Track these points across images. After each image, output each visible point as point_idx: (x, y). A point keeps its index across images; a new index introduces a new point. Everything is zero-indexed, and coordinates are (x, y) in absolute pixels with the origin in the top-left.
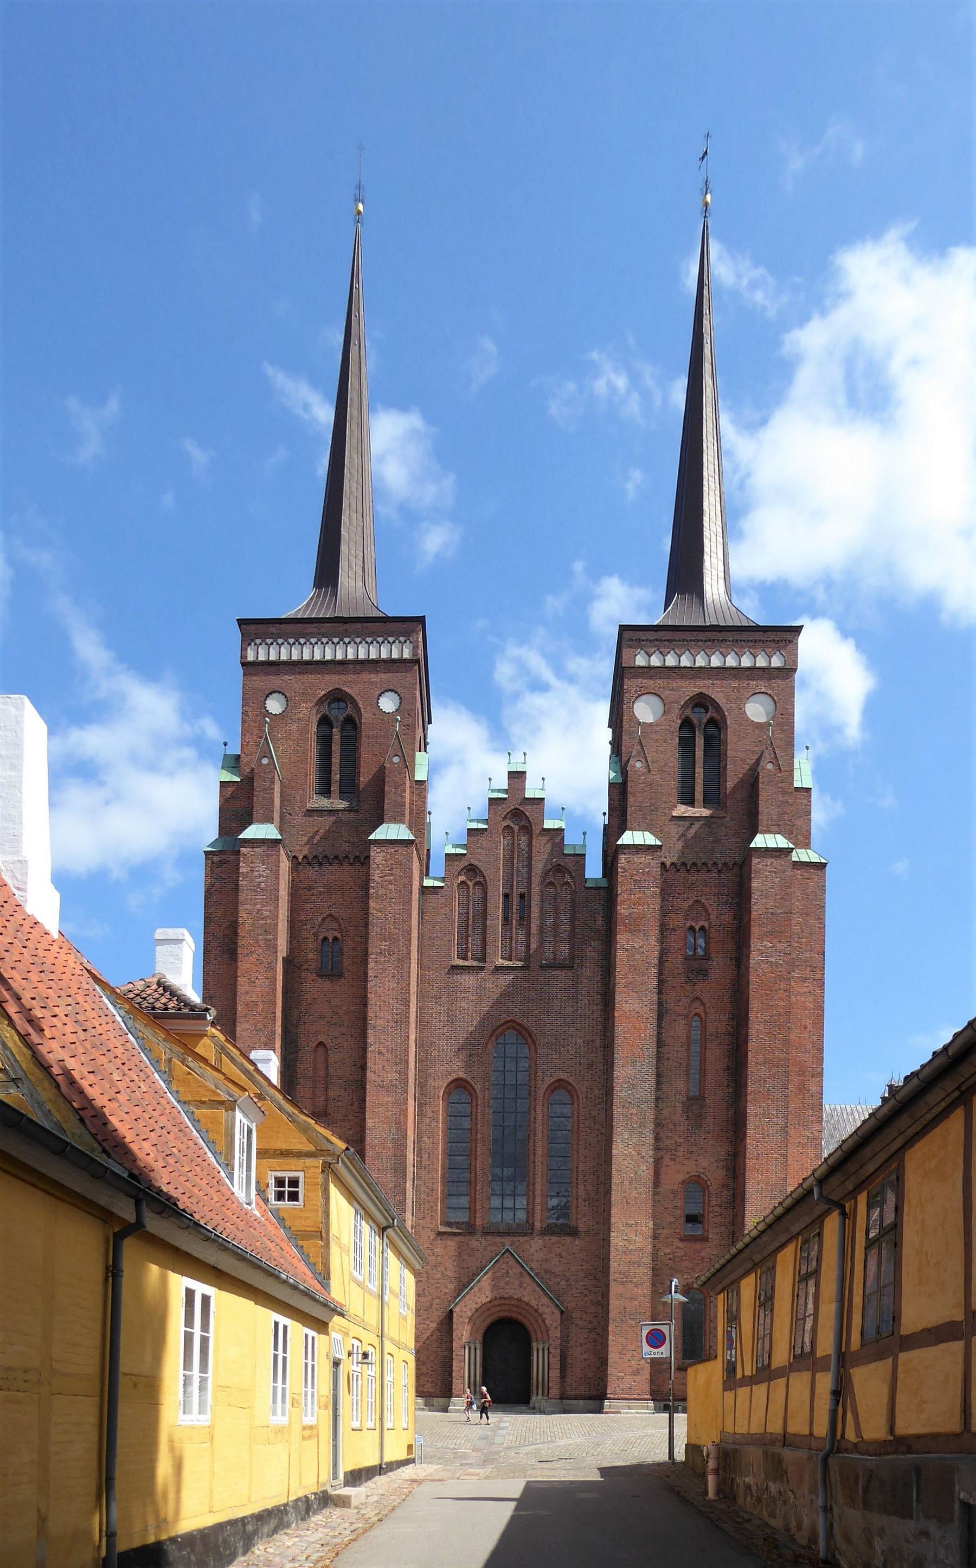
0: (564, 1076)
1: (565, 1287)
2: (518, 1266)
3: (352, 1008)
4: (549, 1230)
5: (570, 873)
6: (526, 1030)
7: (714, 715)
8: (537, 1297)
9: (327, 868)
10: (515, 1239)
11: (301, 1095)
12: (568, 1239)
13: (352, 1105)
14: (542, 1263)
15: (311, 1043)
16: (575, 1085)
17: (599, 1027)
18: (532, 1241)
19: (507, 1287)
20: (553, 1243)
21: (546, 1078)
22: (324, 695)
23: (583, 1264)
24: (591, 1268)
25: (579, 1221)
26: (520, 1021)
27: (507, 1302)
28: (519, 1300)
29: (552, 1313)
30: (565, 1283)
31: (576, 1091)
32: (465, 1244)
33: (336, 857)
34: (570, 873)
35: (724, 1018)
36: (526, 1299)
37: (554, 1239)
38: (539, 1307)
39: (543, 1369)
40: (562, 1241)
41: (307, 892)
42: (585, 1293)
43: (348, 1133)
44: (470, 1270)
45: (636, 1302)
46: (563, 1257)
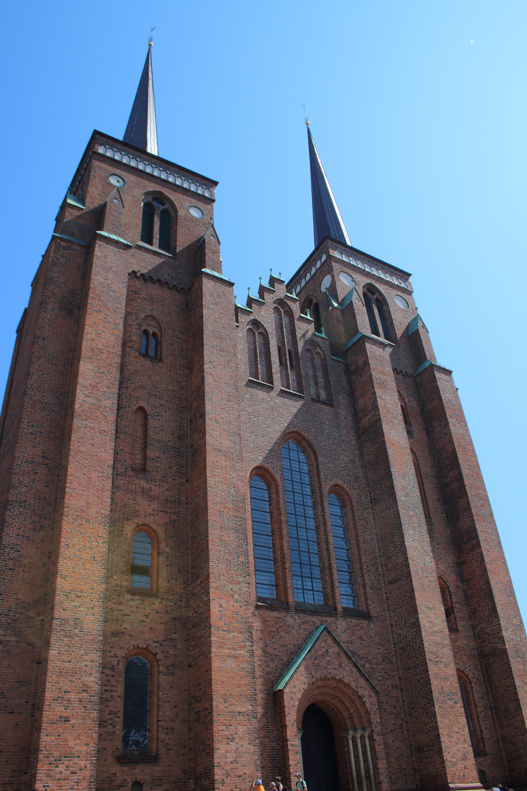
0: (340, 482)
1: (370, 670)
2: (335, 645)
3: (170, 388)
4: (348, 613)
5: (320, 348)
6: (307, 441)
7: (379, 297)
8: (355, 679)
9: (149, 285)
10: (324, 619)
11: (121, 448)
12: (365, 623)
13: (170, 468)
14: (348, 644)
15: (132, 406)
16: (348, 491)
17: (357, 452)
18: (338, 623)
19: (329, 666)
20: (354, 626)
21: (327, 481)
22: (151, 191)
23: (380, 647)
24: (385, 652)
25: (370, 607)
26: (303, 433)
27: (328, 683)
28: (340, 681)
29: (370, 696)
30: (369, 666)
31: (348, 495)
32: (282, 620)
33: (159, 280)
34: (320, 348)
35: (429, 465)
36: (346, 680)
37: (355, 621)
38: (359, 690)
39: (366, 761)
40: (361, 624)
41: (133, 295)
42: (386, 677)
43: (166, 493)
44: (288, 648)
45: (449, 682)
46: (363, 640)
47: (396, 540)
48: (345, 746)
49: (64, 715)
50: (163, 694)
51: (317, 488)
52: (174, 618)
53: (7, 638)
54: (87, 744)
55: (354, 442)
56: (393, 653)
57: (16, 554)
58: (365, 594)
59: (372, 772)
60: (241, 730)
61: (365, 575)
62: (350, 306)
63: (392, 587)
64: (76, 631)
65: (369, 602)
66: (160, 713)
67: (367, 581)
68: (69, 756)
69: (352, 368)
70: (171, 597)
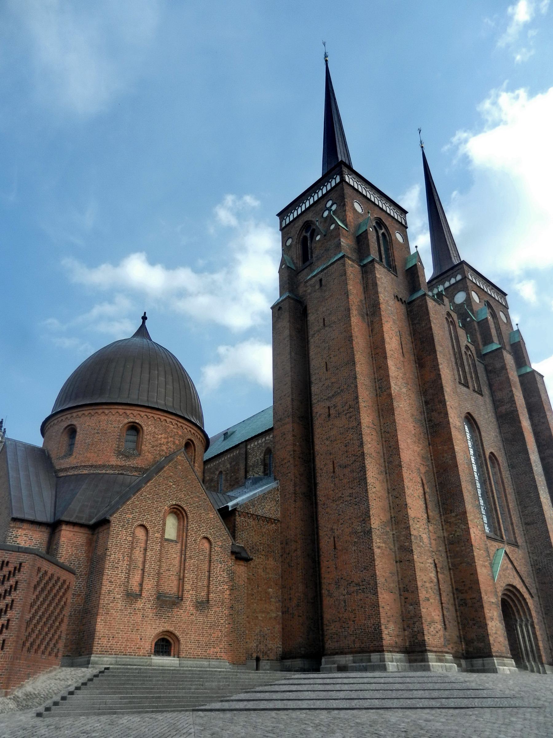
0: (493, 451)
13: (420, 434)
25: (517, 539)
39: (530, 641)
47: (532, 496)
48: (514, 630)
49: (427, 596)
50: (442, 586)
51: (482, 454)
52: (439, 537)
53: (381, 545)
54: (439, 616)
55: (495, 423)
56: (531, 572)
57: (374, 490)
58: (513, 529)
59: (534, 648)
60: (495, 614)
61: (512, 517)
62: (484, 321)
63: (528, 527)
64: (421, 543)
65: (516, 535)
66: (442, 598)
67: (514, 521)
68: (433, 622)
69: (490, 368)
70: (435, 523)
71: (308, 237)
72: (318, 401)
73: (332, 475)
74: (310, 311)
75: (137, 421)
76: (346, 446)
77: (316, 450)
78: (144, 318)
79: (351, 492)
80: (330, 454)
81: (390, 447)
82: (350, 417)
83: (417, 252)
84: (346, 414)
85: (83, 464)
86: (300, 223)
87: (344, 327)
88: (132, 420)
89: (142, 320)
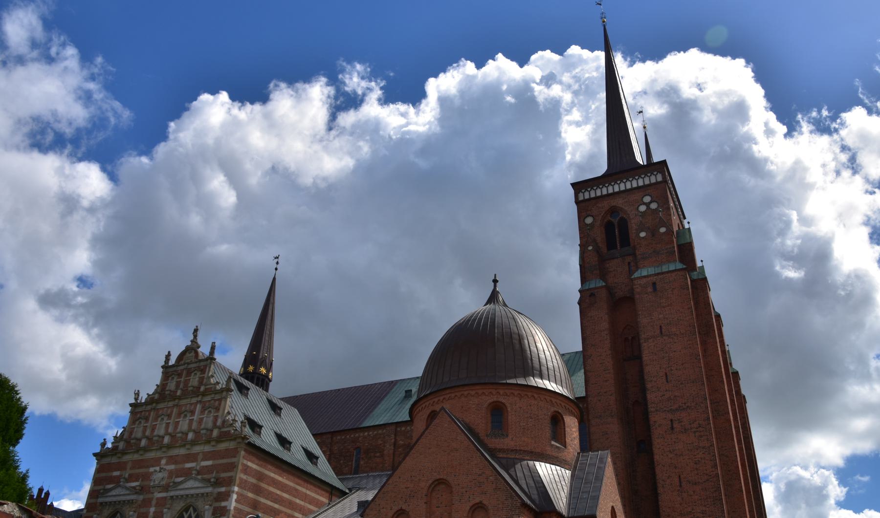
71: (616, 224)
72: (657, 410)
73: (679, 488)
74: (640, 313)
75: (560, 411)
76: (696, 463)
77: (655, 460)
78: (495, 281)
79: (704, 508)
80: (676, 467)
81: (729, 471)
82: (701, 436)
83: (703, 266)
84: (695, 432)
85: (522, 448)
86: (606, 205)
87: (689, 342)
88: (556, 409)
89: (493, 283)
